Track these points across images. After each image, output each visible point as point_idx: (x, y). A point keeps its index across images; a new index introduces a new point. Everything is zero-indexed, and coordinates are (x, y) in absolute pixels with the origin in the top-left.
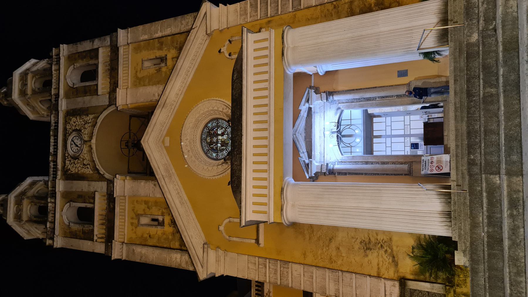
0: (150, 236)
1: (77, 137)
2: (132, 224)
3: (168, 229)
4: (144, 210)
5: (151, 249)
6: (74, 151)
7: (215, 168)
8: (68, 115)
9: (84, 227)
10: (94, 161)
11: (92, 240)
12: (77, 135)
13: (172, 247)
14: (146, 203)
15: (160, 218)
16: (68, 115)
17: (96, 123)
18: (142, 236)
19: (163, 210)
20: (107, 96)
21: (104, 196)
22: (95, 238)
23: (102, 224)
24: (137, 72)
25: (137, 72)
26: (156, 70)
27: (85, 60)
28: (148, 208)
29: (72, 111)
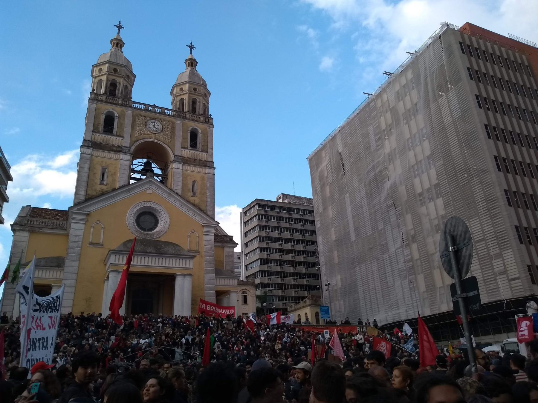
0: (95, 174)
1: (158, 128)
2: (102, 162)
3: (99, 188)
4: (110, 171)
5: (86, 174)
6: (150, 125)
7: (132, 221)
8: (172, 123)
9: (102, 125)
10: (143, 139)
11: (93, 131)
12: (160, 128)
13: (88, 188)
14: (115, 174)
15: (105, 182)
16: (172, 123)
17: (165, 144)
18: (94, 168)
19: (110, 185)
20: (180, 155)
21: (121, 144)
22: (94, 134)
23: (103, 140)
24: (191, 176)
25: (191, 176)
26: (190, 189)
27: (203, 141)
28: (112, 175)
29: (174, 126)
